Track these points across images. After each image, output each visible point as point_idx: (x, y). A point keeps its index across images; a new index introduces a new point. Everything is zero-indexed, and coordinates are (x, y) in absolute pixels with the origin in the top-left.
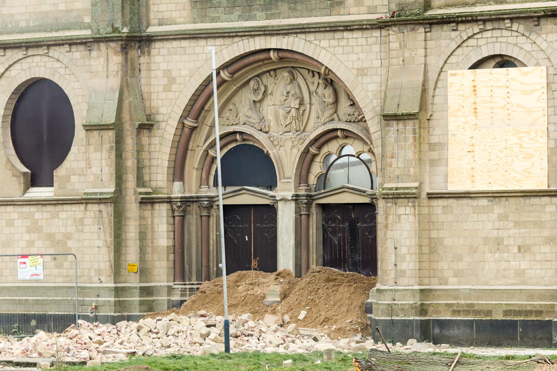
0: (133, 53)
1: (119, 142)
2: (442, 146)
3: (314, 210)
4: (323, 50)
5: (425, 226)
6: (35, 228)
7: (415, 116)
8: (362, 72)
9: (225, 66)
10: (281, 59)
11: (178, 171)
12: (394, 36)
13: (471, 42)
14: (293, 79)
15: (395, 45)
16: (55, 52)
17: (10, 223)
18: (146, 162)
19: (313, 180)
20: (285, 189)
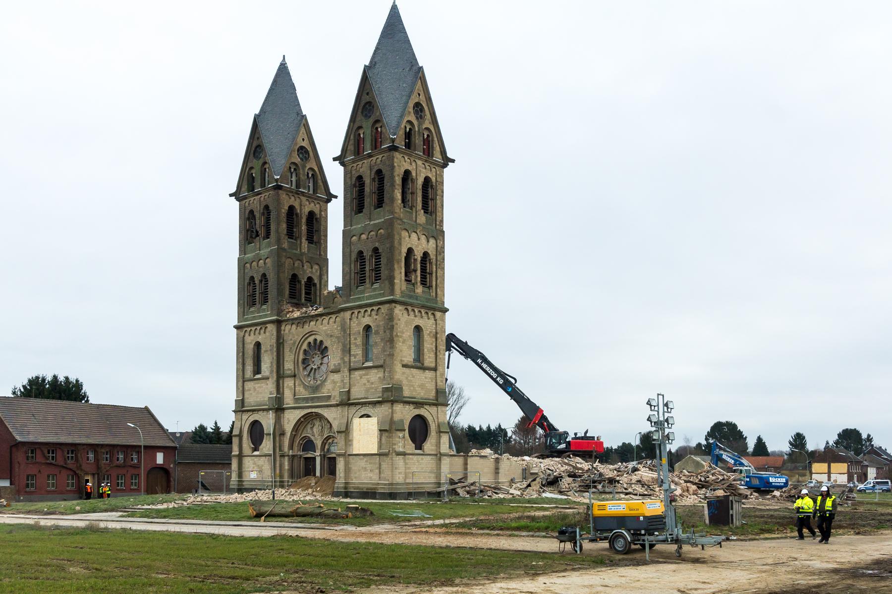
0: (279, 413)
2: (352, 440)
4: (325, 412)
5: (347, 464)
6: (254, 464)
7: (346, 431)
8: (334, 419)
11: (291, 447)
16: (260, 413)
20: (318, 453)
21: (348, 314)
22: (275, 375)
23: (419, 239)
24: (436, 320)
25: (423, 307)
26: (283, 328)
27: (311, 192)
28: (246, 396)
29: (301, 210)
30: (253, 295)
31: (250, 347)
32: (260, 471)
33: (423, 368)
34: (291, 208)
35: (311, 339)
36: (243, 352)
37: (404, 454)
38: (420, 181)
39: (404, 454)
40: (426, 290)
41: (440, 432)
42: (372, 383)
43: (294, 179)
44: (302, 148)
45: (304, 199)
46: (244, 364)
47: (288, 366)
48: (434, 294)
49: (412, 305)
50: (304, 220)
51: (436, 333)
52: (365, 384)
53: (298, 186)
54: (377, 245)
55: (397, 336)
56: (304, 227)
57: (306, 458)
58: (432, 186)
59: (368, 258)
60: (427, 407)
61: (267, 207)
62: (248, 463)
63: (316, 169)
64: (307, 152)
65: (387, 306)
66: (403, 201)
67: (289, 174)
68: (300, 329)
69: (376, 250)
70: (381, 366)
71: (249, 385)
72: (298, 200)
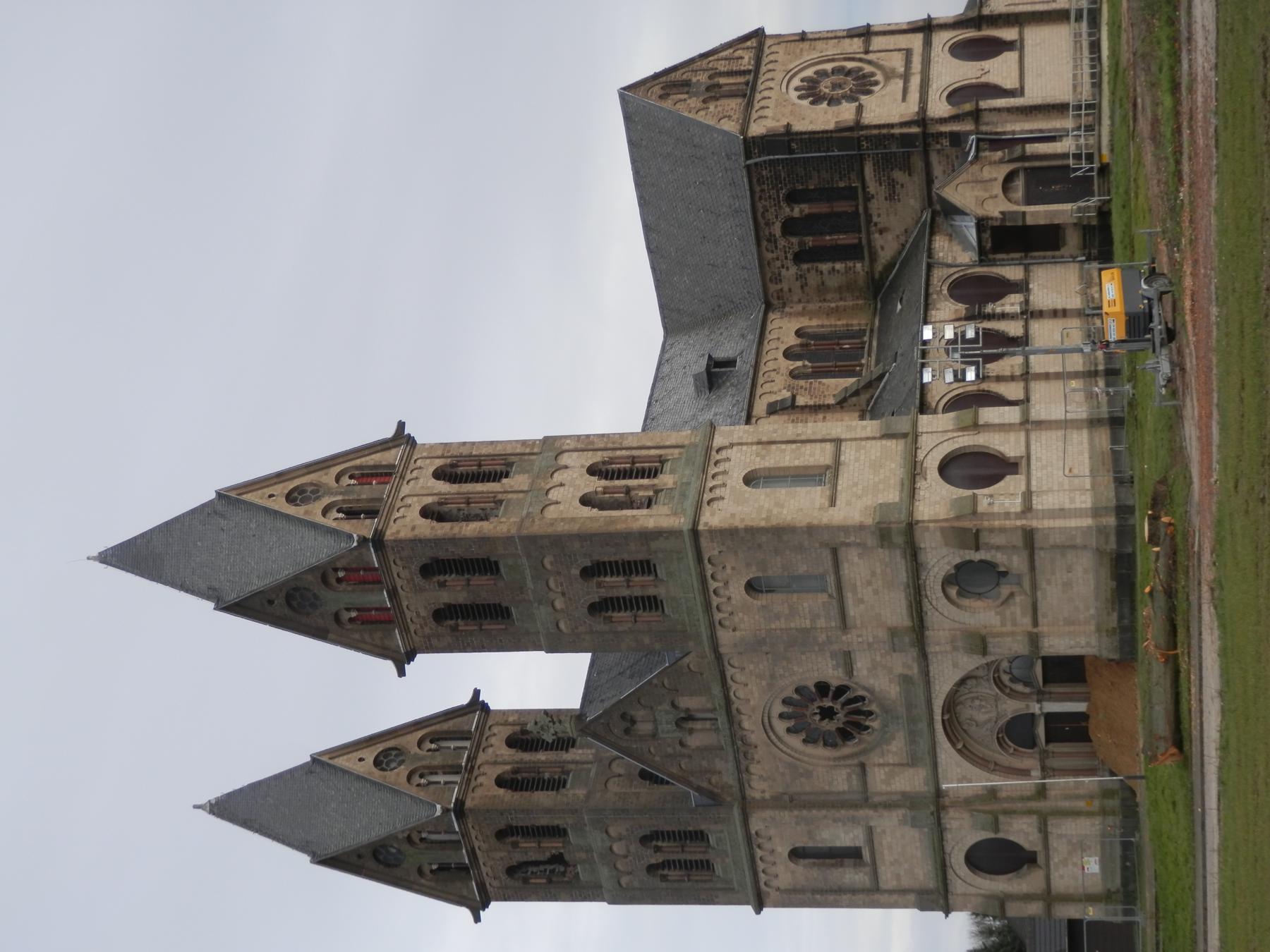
0: (947, 801)
1: (1007, 812)
3: (1047, 689)
6: (1064, 862)
8: (955, 665)
9: (953, 744)
10: (949, 711)
11: (1025, 773)
12: (931, 649)
13: (934, 603)
14: (961, 703)
15: (937, 648)
16: (948, 849)
17: (1062, 877)
18: (1019, 793)
19: (1027, 690)
20: (1035, 708)
21: (725, 636)
22: (862, 813)
23: (562, 485)
24: (732, 445)
25: (704, 470)
26: (757, 795)
27: (467, 744)
28: (906, 882)
29: (505, 763)
30: (689, 866)
31: (801, 873)
32: (1080, 847)
33: (835, 467)
34: (501, 782)
35: (781, 726)
36: (814, 891)
37: (1028, 495)
38: (443, 487)
39: (1028, 495)
40: (667, 467)
41: (976, 426)
42: (873, 574)
43: (442, 778)
44: (377, 763)
45: (482, 757)
46: (840, 890)
47: (841, 781)
48: (677, 451)
49: (701, 493)
50: (527, 756)
51: (759, 443)
52: (876, 592)
53: (455, 770)
54: (576, 572)
55: (768, 519)
56: (542, 756)
57: (1048, 741)
58: (453, 466)
59: (604, 593)
60: (921, 455)
61: (501, 834)
62: (1063, 879)
63: (420, 734)
64: (385, 753)
65: (704, 542)
66: (485, 518)
67: (432, 787)
68: (759, 754)
69: (587, 573)
70: (835, 552)
71: (887, 878)
72: (485, 769)
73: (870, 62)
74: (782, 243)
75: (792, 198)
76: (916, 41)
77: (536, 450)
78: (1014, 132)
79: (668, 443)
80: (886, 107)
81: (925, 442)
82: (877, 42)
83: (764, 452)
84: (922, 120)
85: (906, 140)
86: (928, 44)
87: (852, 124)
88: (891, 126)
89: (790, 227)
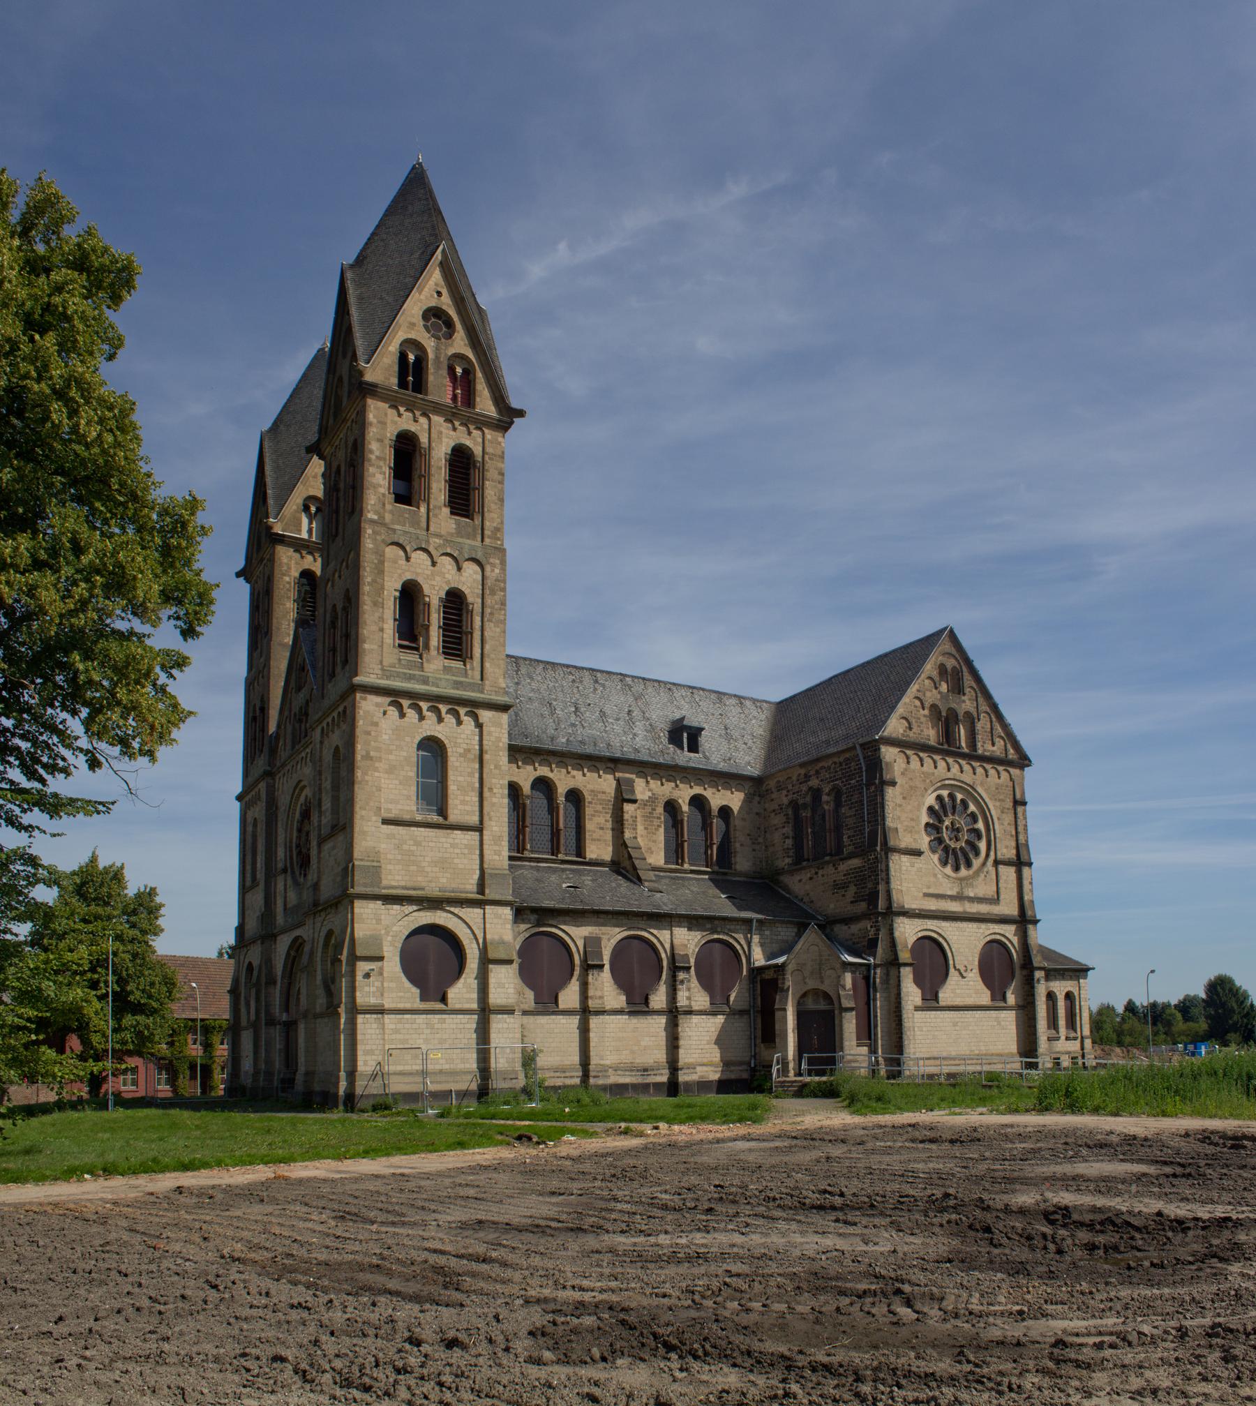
23: (434, 564)
48: (477, 674)
55: (367, 757)
73: (984, 864)
74: (804, 788)
75: (837, 793)
76: (1009, 907)
77: (487, 541)
78: (875, 1000)
79: (487, 665)
80: (915, 879)
81: (472, 914)
82: (1009, 873)
83: (471, 756)
84: (892, 912)
85: (872, 898)
86: (1004, 920)
87: (891, 843)
88: (888, 882)
89: (816, 794)
